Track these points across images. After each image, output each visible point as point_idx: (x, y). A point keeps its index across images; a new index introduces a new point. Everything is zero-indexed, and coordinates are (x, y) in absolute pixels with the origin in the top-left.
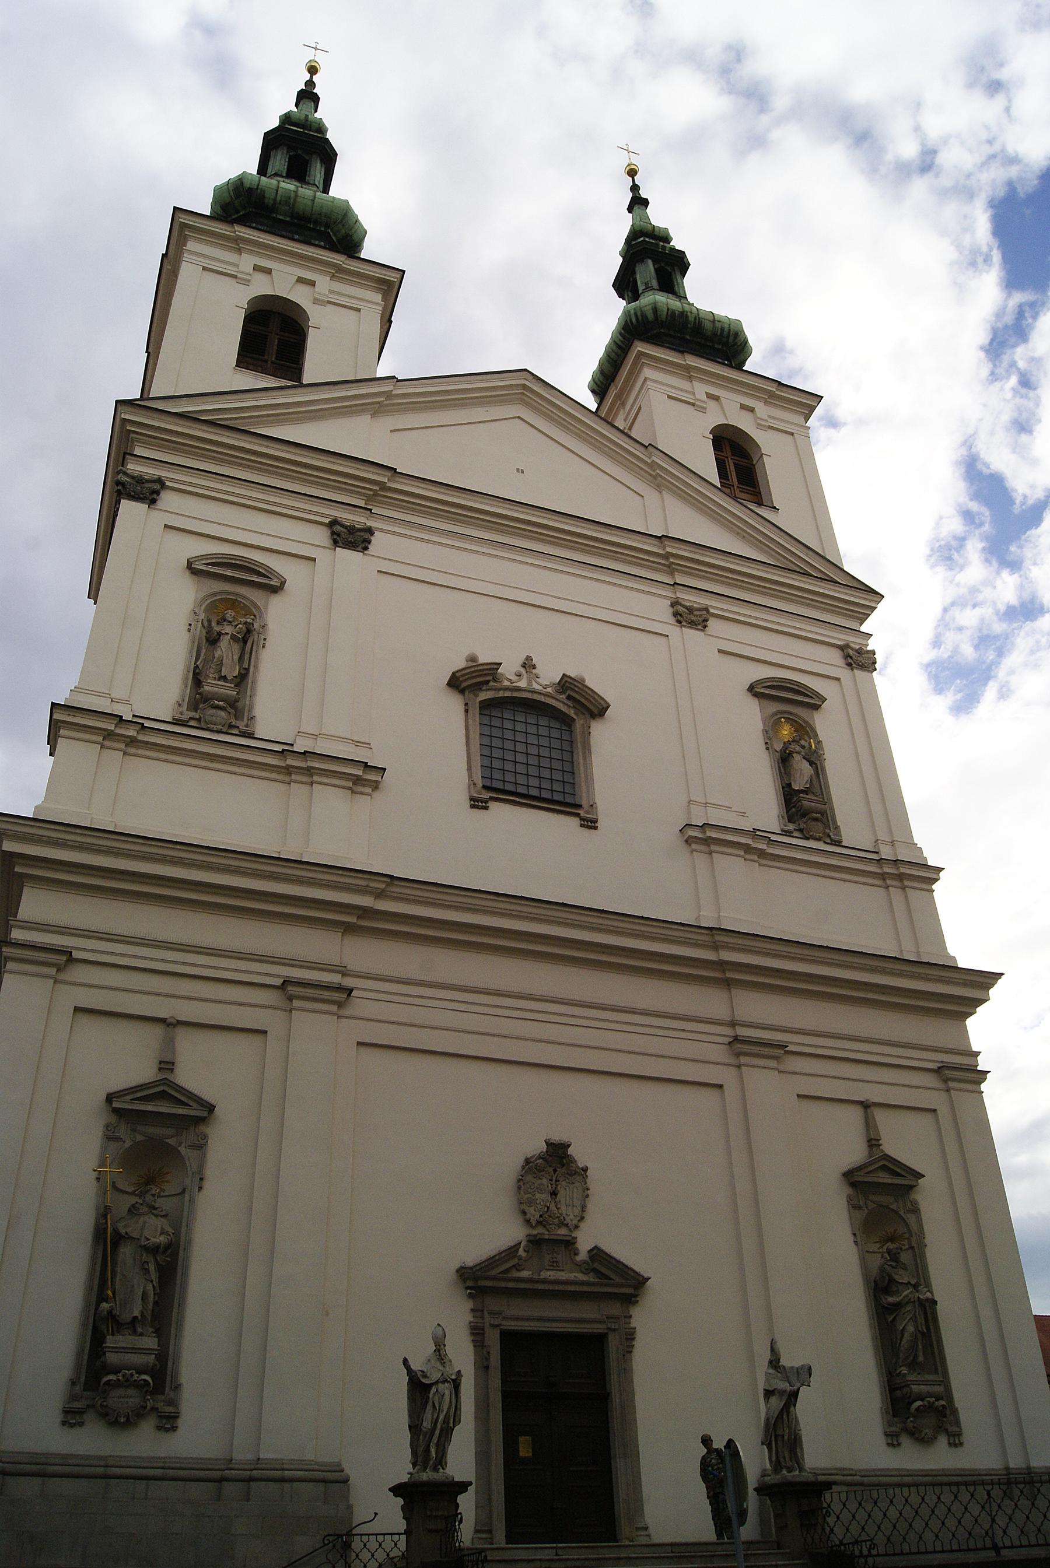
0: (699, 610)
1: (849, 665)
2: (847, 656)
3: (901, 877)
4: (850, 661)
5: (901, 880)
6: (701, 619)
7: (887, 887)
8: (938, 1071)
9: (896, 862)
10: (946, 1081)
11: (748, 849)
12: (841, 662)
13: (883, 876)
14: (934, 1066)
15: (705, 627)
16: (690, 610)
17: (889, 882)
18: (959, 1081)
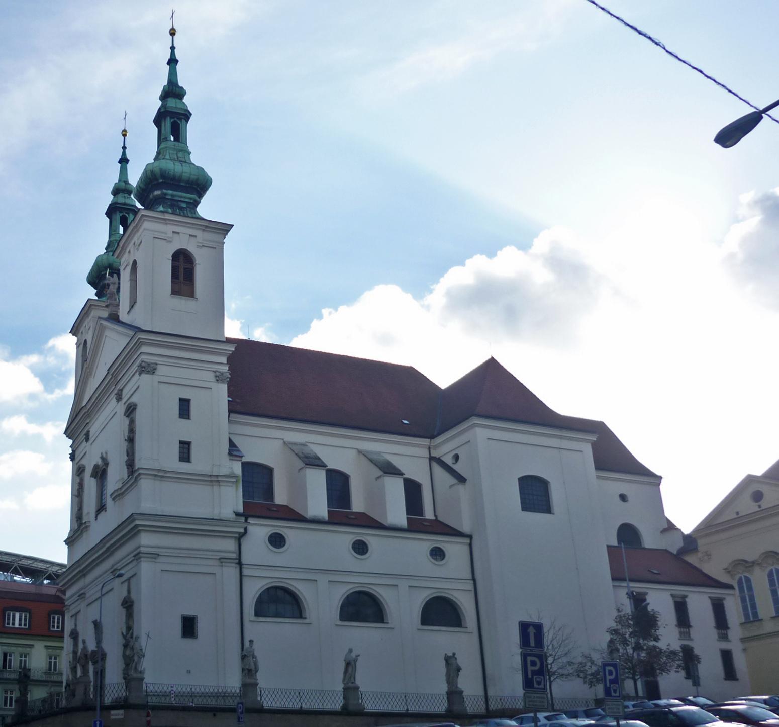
0: (152, 363)
1: (217, 380)
2: (216, 376)
3: (218, 481)
4: (217, 378)
5: (219, 482)
6: (152, 369)
7: (213, 485)
8: (220, 559)
9: (217, 476)
10: (222, 562)
11: (156, 475)
12: (213, 379)
13: (211, 481)
14: (218, 557)
15: (154, 372)
16: (149, 364)
17: (214, 483)
18: (225, 562)
